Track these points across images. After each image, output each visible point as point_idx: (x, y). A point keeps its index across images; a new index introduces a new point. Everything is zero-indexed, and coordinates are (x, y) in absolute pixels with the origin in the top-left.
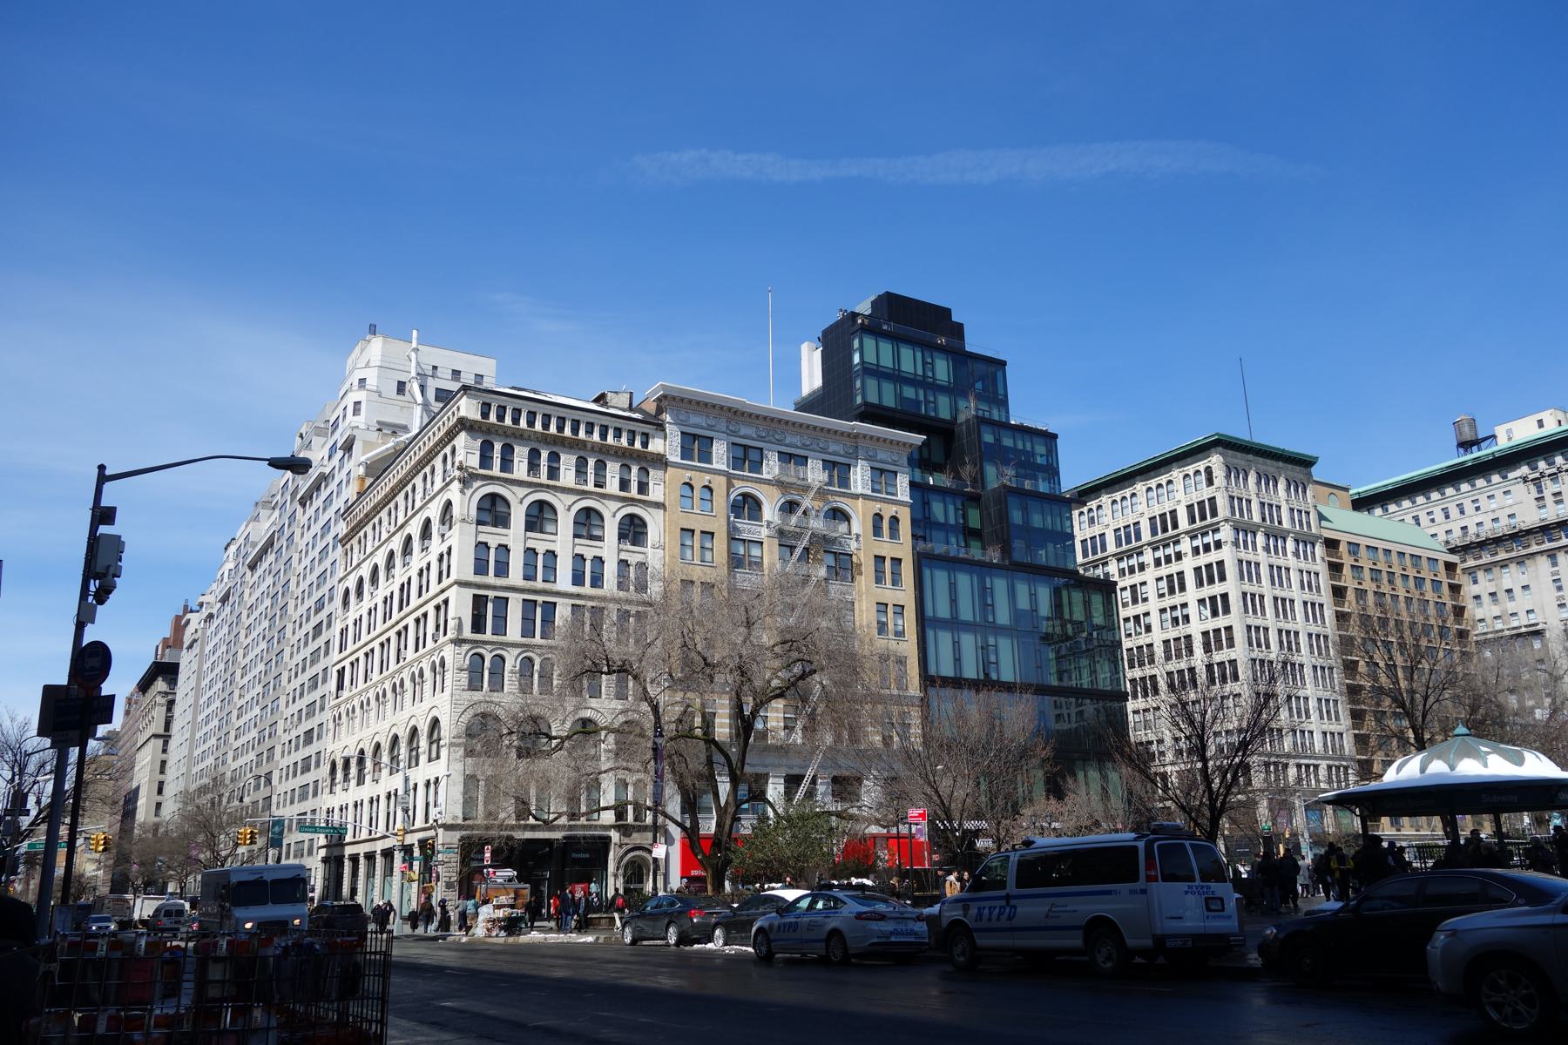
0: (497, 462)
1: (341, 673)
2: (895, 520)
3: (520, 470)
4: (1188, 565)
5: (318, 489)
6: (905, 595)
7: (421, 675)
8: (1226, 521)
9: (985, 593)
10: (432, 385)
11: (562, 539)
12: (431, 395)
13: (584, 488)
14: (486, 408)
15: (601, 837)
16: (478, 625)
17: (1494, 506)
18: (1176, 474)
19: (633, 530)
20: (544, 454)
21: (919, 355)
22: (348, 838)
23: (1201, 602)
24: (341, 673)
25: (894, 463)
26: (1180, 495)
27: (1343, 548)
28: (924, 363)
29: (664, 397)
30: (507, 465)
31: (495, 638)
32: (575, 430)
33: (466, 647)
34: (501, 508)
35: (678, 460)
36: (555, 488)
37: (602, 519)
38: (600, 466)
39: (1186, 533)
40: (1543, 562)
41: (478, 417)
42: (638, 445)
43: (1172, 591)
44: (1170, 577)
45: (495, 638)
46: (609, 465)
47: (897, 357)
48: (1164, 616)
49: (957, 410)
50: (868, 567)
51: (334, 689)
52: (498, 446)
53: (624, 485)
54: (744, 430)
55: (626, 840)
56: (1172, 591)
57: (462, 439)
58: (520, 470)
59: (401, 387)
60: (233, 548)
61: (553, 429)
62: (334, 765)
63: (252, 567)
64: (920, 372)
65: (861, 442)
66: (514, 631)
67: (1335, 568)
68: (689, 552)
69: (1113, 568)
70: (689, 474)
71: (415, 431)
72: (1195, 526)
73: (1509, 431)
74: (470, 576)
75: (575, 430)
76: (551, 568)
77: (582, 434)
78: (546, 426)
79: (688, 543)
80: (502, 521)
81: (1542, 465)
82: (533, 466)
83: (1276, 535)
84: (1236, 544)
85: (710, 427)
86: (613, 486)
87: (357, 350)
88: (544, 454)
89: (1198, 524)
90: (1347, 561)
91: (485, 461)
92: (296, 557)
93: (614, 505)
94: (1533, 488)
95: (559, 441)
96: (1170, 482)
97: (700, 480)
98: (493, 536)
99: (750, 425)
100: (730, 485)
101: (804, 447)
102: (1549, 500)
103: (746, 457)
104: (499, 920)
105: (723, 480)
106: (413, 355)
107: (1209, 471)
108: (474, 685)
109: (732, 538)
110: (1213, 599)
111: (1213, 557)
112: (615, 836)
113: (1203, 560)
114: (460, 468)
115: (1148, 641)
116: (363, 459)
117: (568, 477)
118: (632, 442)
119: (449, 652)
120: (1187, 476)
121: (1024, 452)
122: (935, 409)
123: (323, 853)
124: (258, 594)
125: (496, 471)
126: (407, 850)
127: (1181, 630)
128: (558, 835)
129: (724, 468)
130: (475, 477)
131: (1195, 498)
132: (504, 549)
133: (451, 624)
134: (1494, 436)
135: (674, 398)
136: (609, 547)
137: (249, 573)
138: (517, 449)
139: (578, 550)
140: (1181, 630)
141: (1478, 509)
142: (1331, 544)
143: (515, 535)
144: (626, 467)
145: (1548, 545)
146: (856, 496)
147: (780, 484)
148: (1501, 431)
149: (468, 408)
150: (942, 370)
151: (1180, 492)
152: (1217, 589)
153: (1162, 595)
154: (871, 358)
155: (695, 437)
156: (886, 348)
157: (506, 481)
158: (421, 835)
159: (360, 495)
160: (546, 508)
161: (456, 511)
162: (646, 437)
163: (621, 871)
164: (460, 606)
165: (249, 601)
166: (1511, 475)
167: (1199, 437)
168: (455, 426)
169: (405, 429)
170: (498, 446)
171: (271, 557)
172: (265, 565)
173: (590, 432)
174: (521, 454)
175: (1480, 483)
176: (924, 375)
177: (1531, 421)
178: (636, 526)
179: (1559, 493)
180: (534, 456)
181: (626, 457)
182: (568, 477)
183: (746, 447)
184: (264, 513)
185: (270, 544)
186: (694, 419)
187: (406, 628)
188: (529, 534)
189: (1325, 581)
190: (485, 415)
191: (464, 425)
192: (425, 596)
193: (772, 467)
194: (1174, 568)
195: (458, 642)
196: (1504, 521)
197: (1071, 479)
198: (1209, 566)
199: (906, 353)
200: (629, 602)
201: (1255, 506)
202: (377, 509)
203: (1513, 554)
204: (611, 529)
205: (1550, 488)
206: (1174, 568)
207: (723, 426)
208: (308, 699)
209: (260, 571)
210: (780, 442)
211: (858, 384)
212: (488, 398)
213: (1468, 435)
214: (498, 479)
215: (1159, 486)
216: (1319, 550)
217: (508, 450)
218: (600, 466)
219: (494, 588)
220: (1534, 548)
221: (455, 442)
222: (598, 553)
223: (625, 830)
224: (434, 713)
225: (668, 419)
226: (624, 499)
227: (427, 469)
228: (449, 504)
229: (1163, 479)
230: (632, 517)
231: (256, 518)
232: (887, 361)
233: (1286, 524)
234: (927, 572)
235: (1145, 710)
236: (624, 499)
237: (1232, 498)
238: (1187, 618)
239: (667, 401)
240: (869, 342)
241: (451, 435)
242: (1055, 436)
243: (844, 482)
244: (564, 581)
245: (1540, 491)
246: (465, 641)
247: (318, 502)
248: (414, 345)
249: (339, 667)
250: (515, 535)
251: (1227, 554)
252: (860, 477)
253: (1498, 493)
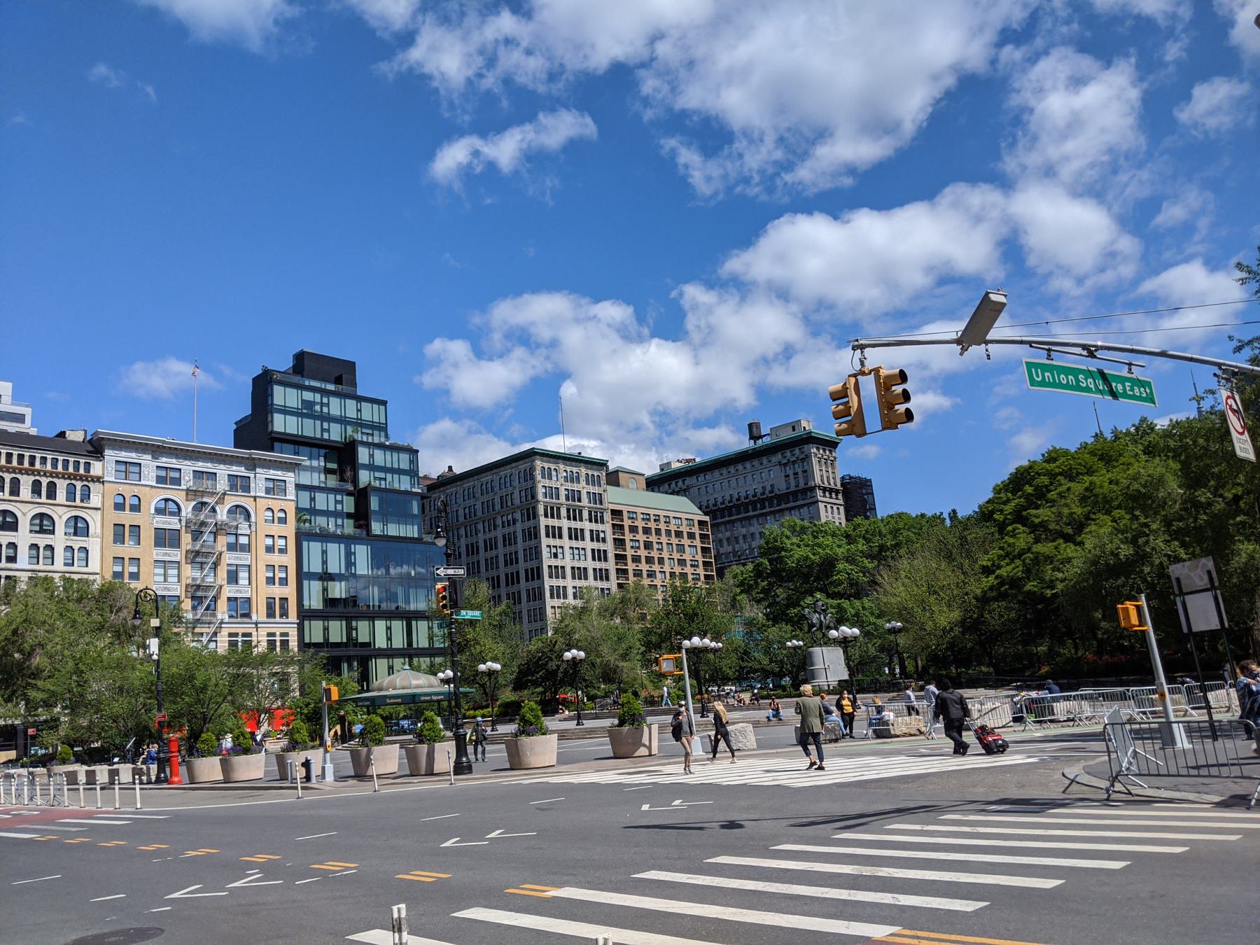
6: (289, 559)
9: (349, 554)
19: (79, 527)
67: (618, 528)
90: (627, 523)
93: (60, 510)
142: (616, 513)
189: (610, 537)
220: (783, 506)
234: (305, 544)
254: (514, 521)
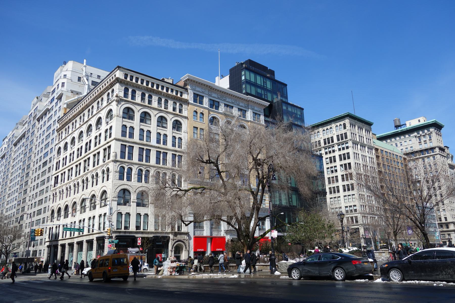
0: (130, 96)
1: (57, 178)
3: (138, 99)
4: (337, 154)
5: (42, 118)
7: (70, 188)
8: (350, 140)
10: (91, 79)
11: (153, 126)
12: (90, 83)
13: (160, 108)
14: (126, 76)
15: (167, 237)
16: (123, 156)
17: (406, 144)
18: (333, 125)
19: (177, 125)
20: (147, 95)
21: (262, 79)
22: (60, 238)
23: (341, 165)
24: (57, 178)
25: (259, 111)
26: (334, 132)
27: (379, 151)
28: (264, 82)
29: (188, 79)
30: (133, 97)
31: (129, 161)
32: (158, 87)
33: (118, 163)
34: (131, 113)
35: (192, 102)
36: (151, 108)
37: (167, 121)
38: (166, 102)
39: (323, 147)
40: (420, 160)
41: (123, 78)
42: (179, 95)
43: (331, 162)
44: (330, 158)
45: (129, 161)
46: (169, 102)
47: (256, 79)
48: (328, 170)
49: (273, 99)
51: (53, 184)
52: (130, 90)
53: (174, 109)
54: (214, 95)
55: (175, 238)
56: (331, 162)
57: (117, 87)
58: (138, 99)
59: (79, 79)
60: (7, 140)
61: (150, 86)
62: (53, 211)
63: (15, 145)
64: (262, 85)
65: (250, 103)
66: (136, 158)
67: (378, 157)
68: (196, 135)
69: (323, 151)
70: (196, 108)
71: (86, 94)
72: (326, 145)
73: (410, 123)
74: (120, 137)
75: (158, 87)
76: (149, 137)
77: (160, 89)
78: (147, 84)
79: (196, 132)
80: (131, 118)
81: (421, 132)
82: (143, 99)
83: (363, 146)
84: (353, 147)
85: (203, 92)
86: (170, 109)
87: (59, 70)
88: (147, 95)
89: (327, 145)
91: (126, 95)
92: (35, 139)
94: (418, 139)
95: (151, 91)
96: (331, 128)
98: (128, 123)
99: (215, 93)
100: (209, 113)
101: (232, 103)
102: (423, 143)
104: (174, 268)
105: (207, 111)
106: (84, 68)
107: (344, 125)
108: (121, 178)
110: (345, 165)
111: (346, 151)
112: (171, 236)
113: (342, 152)
114: (117, 96)
115: (336, 175)
116: (66, 102)
117: (155, 104)
118: (177, 94)
119: (111, 166)
120: (324, 130)
121: (294, 113)
122: (267, 97)
123: (48, 244)
124: (18, 154)
125: (129, 99)
126: (90, 242)
127: (334, 174)
128: (151, 236)
129: (207, 107)
130: (122, 100)
131: (339, 133)
132: (132, 128)
133: (112, 155)
134: (406, 124)
135: (191, 80)
136: (169, 131)
137: (37, 123)
138: (137, 92)
139: (159, 131)
140: (334, 174)
141: (401, 145)
142: (377, 150)
143: (136, 123)
144: (175, 103)
145: (422, 156)
146: (248, 121)
147: (225, 115)
148: (407, 123)
149: (119, 74)
150: (269, 85)
151: (335, 131)
152: (347, 161)
153: (328, 163)
154: (248, 78)
155: (198, 95)
156: (252, 75)
157: (133, 103)
158: (97, 235)
159: (65, 114)
160: (147, 115)
161: (114, 113)
162: (182, 93)
163: (174, 249)
164: (116, 148)
165: (13, 156)
166: (411, 135)
167: (342, 114)
168: (115, 81)
169: (81, 93)
170: (130, 90)
171: (24, 140)
172: (21, 143)
173: (163, 88)
174: (138, 94)
175: (402, 137)
176: (264, 86)
177: (416, 120)
178: (178, 124)
179: (426, 141)
180: (143, 95)
181: (175, 99)
182: (155, 104)
183: (213, 101)
184: (20, 127)
185: (23, 136)
186: (198, 89)
187: (65, 172)
188: (141, 124)
190: (126, 78)
191: (118, 80)
192: (72, 162)
193: (222, 109)
194: (332, 155)
195: (115, 161)
196: (409, 149)
197: (309, 121)
198: (344, 154)
199: (258, 78)
200: (176, 151)
201: (357, 136)
202: (75, 117)
203: (411, 158)
204: (170, 124)
205: (423, 139)
206: (332, 155)
207: (207, 92)
208: (40, 189)
209: (18, 146)
210: (225, 100)
211: (244, 86)
212: (127, 72)
213: (398, 124)
214: (130, 102)
215: (327, 129)
216: (374, 151)
217: (134, 92)
218: (166, 102)
219: (129, 142)
220: (418, 157)
221: (114, 88)
222: (165, 133)
223: (176, 234)
224: (104, 189)
225: (189, 87)
226: (174, 114)
227: (100, 100)
228: (111, 110)
229: (329, 127)
230: (177, 121)
231: (17, 128)
232: (253, 80)
233: (365, 143)
235: (334, 198)
236: (174, 114)
237: (352, 133)
238: (336, 171)
240: (248, 73)
241: (112, 85)
242: (303, 109)
243: (244, 116)
244: (153, 142)
245: (420, 140)
246: (118, 161)
247: (45, 119)
248: (85, 64)
249: (56, 175)
250: (136, 123)
251: (350, 150)
252: (249, 115)
253: (408, 140)
254: (334, 151)
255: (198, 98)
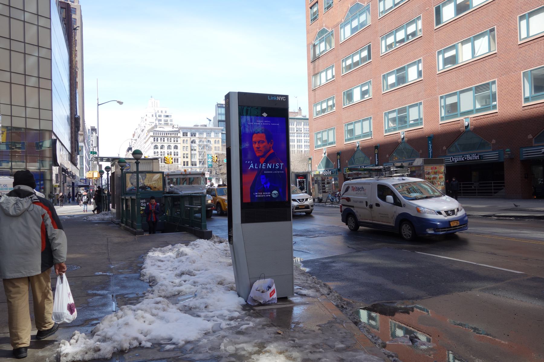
2: (218, 141)
11: (166, 150)
19: (176, 147)
30: (157, 141)
50: (213, 149)
53: (174, 141)
59: (153, 116)
80: (157, 148)
91: (154, 141)
97: (185, 139)
98: (156, 150)
103: (193, 135)
109: (191, 147)
143: (159, 150)
154: (220, 112)
180: (161, 139)
191: (151, 136)
193: (197, 135)
204: (173, 148)
217: (157, 139)
218: (171, 139)
239: (181, 128)
255: (185, 134)
